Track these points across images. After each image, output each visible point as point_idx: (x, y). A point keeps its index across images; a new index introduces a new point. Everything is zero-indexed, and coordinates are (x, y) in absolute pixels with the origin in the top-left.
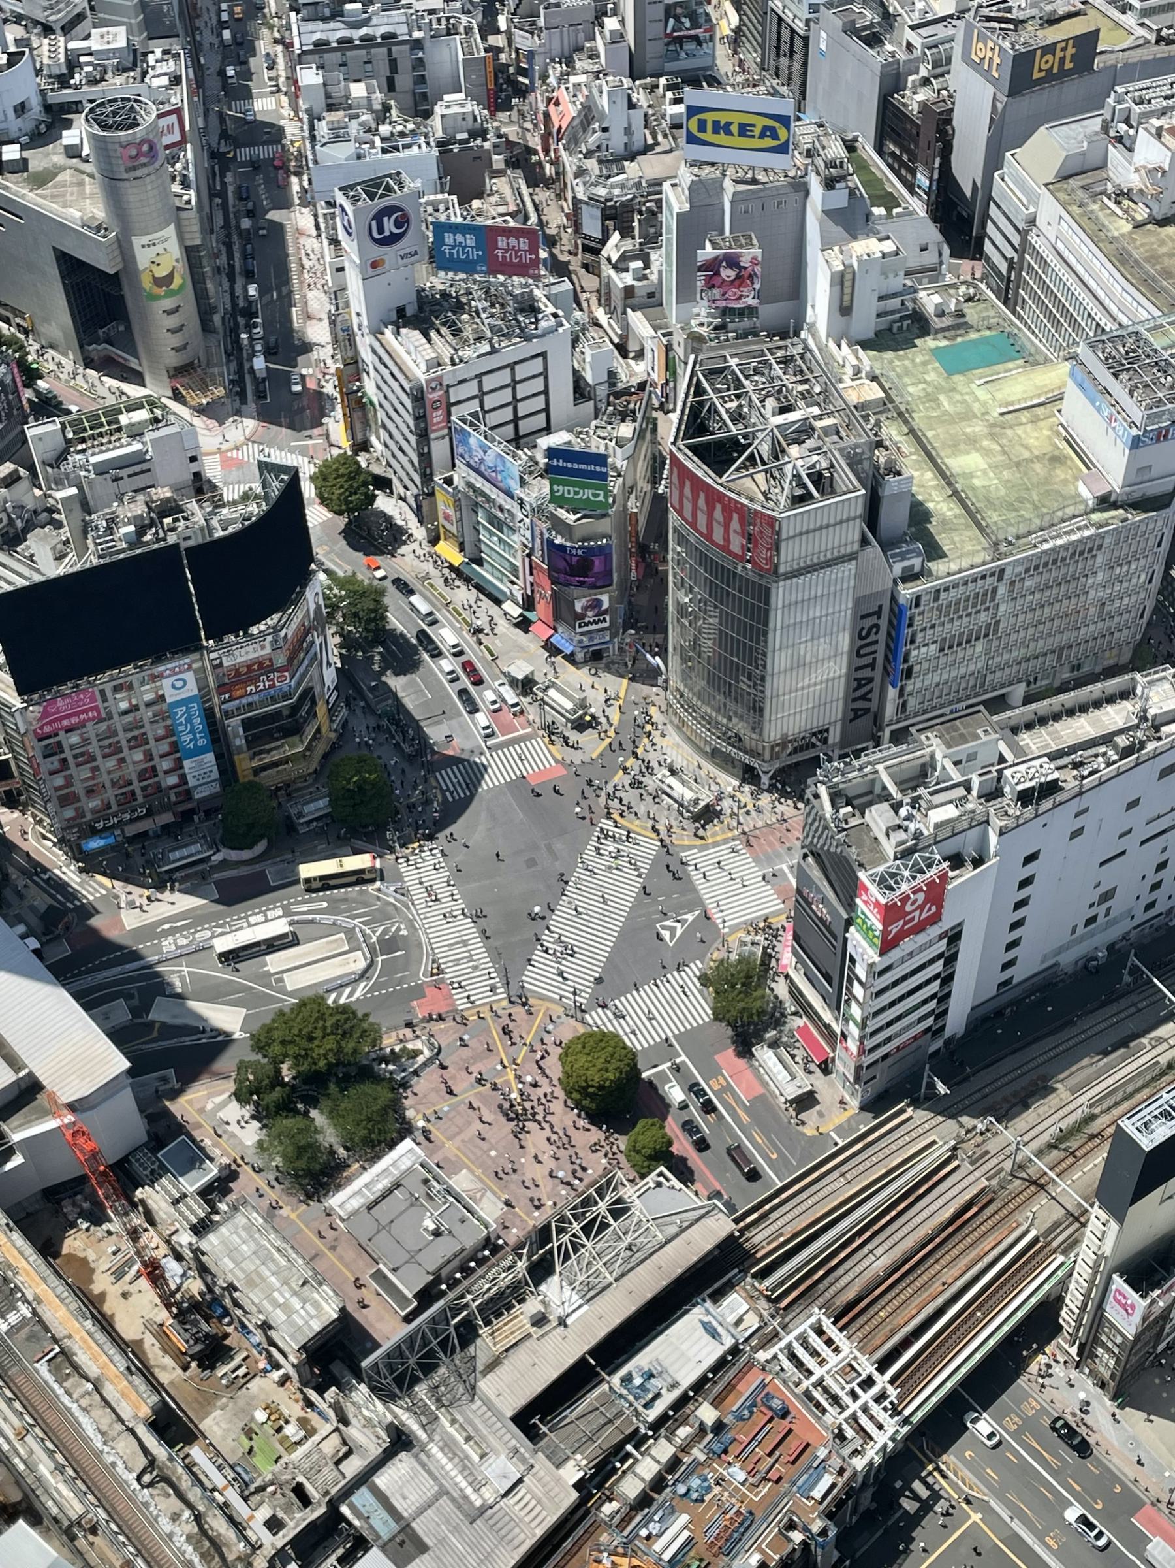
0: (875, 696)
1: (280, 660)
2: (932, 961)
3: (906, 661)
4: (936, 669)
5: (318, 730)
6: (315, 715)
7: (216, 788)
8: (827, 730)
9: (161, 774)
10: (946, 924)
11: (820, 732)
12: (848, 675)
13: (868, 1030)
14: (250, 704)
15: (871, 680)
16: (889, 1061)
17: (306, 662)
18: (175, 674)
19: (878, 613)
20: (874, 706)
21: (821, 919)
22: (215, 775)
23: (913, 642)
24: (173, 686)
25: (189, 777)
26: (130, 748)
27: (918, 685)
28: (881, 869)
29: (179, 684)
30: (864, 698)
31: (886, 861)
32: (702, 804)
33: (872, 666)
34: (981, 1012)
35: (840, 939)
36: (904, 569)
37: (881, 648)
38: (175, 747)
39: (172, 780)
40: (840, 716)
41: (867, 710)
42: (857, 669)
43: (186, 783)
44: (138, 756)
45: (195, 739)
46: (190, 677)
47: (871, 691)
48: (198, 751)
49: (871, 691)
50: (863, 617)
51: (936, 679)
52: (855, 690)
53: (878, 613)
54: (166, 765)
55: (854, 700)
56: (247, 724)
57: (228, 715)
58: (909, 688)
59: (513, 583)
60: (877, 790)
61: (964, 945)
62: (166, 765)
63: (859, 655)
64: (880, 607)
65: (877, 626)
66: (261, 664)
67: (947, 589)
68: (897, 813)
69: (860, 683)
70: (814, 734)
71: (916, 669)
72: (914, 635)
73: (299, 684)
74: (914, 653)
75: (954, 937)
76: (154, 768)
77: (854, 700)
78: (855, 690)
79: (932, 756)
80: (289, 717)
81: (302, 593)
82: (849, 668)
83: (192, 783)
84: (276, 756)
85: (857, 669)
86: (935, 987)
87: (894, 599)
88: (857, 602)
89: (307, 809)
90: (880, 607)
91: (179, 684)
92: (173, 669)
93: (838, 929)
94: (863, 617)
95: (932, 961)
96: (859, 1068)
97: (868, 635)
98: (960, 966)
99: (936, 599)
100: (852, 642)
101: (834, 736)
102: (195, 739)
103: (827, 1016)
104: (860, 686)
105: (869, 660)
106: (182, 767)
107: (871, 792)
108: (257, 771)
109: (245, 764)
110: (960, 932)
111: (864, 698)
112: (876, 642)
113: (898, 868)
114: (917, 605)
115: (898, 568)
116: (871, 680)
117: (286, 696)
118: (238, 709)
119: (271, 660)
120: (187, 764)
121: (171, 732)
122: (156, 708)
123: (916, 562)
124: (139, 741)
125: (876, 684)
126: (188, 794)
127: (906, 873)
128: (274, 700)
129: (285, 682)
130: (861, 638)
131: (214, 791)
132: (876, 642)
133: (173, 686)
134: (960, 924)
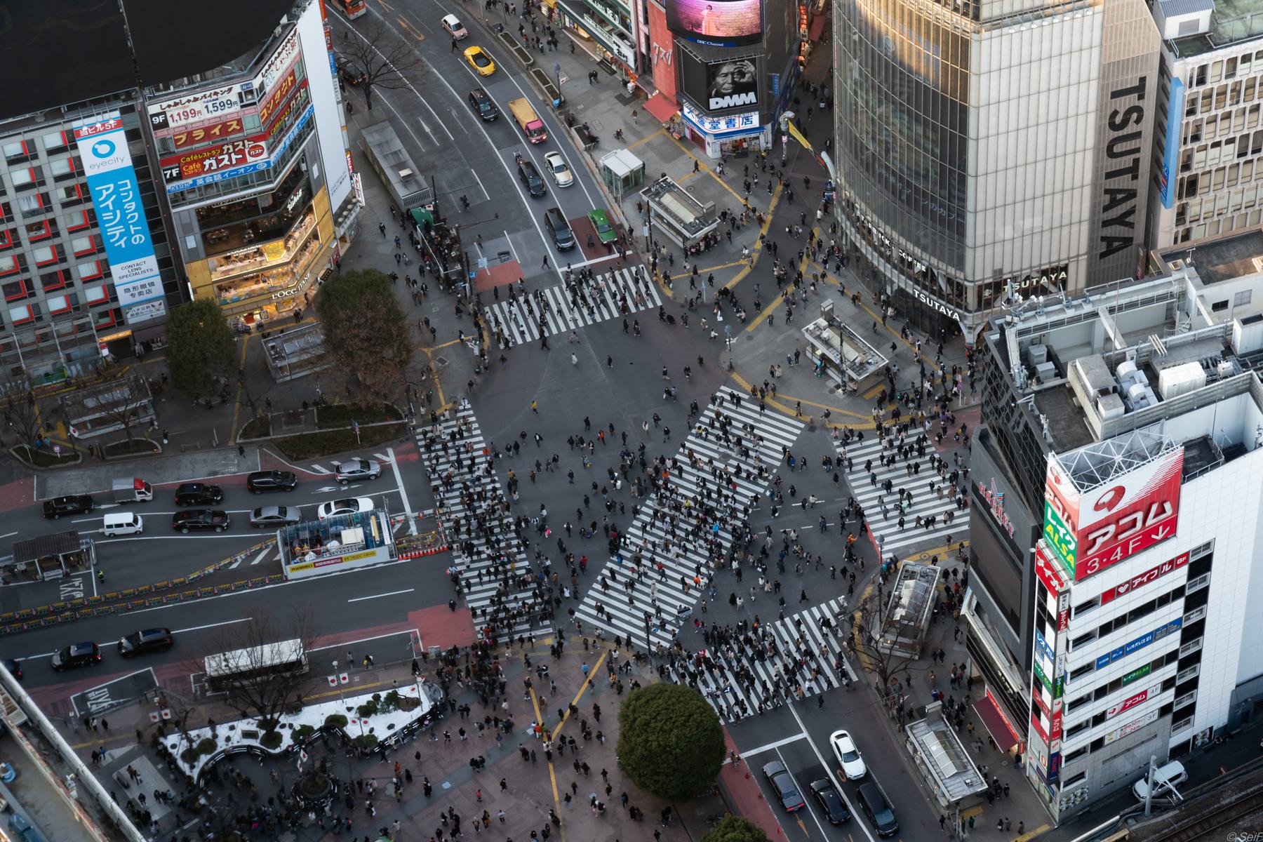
0: (1140, 219)
1: (253, 123)
2: (1164, 600)
3: (1186, 167)
4: (1233, 182)
5: (315, 236)
6: (310, 210)
7: (160, 310)
8: (1065, 269)
9: (78, 284)
10: (1184, 541)
11: (1053, 270)
12: (1095, 185)
13: (1069, 697)
14: (208, 186)
15: (1132, 194)
16: (1102, 753)
17: (295, 130)
18: (96, 132)
19: (1140, 89)
20: (1139, 234)
21: (1002, 529)
22: (159, 290)
23: (1196, 138)
24: (95, 152)
25: (120, 291)
26: (32, 242)
27: (1208, 207)
28: (1082, 450)
29: (104, 149)
30: (1121, 220)
31: (1092, 441)
32: (872, 369)
33: (1133, 171)
34: (1249, 693)
35: (1027, 560)
36: (1183, 26)
37: (1146, 144)
38: (98, 246)
39: (95, 293)
40: (1084, 248)
41: (1128, 241)
42: (1109, 175)
43: (115, 299)
44: (44, 253)
45: (127, 233)
46: (119, 138)
47: (1131, 212)
48: (132, 253)
49: (1131, 212)
50: (1115, 95)
51: (1236, 199)
52: (1106, 209)
53: (1140, 89)
54: (87, 269)
55: (1106, 224)
56: (207, 218)
57: (180, 198)
58: (1192, 211)
59: (622, 36)
60: (1098, 342)
61: (1217, 579)
62: (87, 269)
63: (1111, 153)
64: (1143, 80)
65: (1139, 110)
66: (225, 127)
67: (1246, 58)
68: (1113, 372)
69: (1115, 197)
70: (1044, 273)
71: (1202, 182)
72: (1198, 127)
73: (283, 160)
74: (1198, 157)
75: (1201, 565)
76: (67, 273)
77: (1106, 224)
78: (1106, 209)
79: (1183, 295)
80: (266, 210)
81: (291, 25)
82: (1096, 170)
83: (124, 299)
84: (249, 267)
85: (1109, 175)
86: (1173, 641)
87: (1163, 70)
88: (1106, 71)
89: (288, 348)
90: (1143, 80)
91: (104, 149)
92: (91, 126)
93: (1023, 541)
94: (1115, 95)
95: (1164, 600)
96: (1055, 759)
97: (1125, 123)
98: (1213, 612)
99: (1231, 74)
100: (1099, 131)
101: (1077, 276)
102: (127, 233)
103: (1014, 682)
104: (1113, 203)
105: (1127, 162)
106: (109, 275)
107: (1089, 344)
108: (222, 288)
109: (205, 275)
110: (1210, 557)
111: (1121, 220)
112: (1138, 135)
113: (1107, 451)
114: (1201, 81)
115: (1173, 27)
116: (1132, 194)
117: (263, 176)
118: (192, 191)
119: (239, 122)
120: (116, 270)
121: (92, 220)
122: (71, 183)
123: (1202, 19)
124: (46, 230)
125: (1141, 200)
126: (118, 317)
127: (1118, 458)
128: (246, 184)
129: (263, 159)
130: (1113, 126)
131: (156, 314)
132: (1138, 135)
133: (95, 152)
134: (1207, 546)
